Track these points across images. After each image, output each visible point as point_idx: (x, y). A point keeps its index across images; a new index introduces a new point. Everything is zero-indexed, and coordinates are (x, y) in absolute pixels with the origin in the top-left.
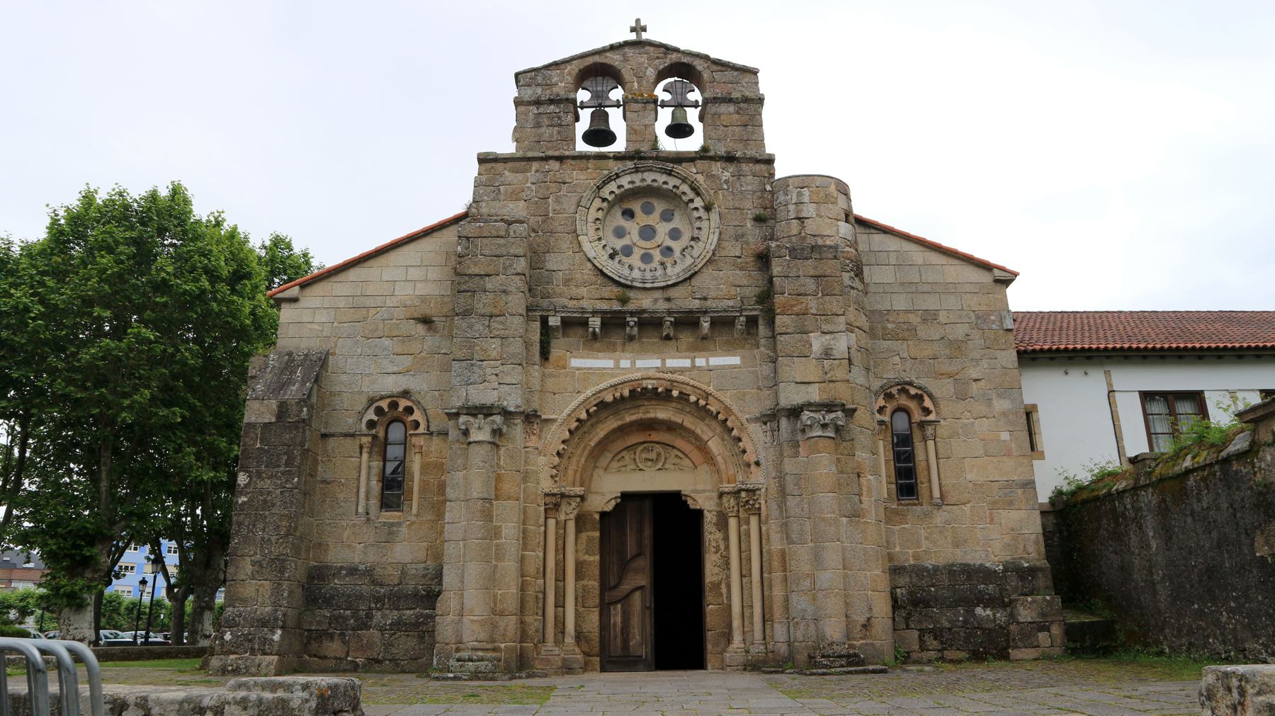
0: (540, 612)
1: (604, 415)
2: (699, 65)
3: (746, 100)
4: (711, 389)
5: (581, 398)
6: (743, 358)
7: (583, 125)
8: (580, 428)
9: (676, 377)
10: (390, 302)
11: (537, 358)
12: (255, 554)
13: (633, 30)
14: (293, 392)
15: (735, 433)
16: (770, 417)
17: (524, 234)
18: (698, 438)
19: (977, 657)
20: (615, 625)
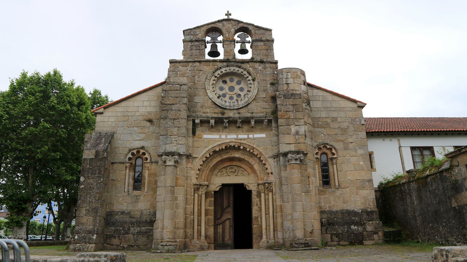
0: (192, 228)
1: (216, 155)
2: (251, 28)
3: (268, 41)
4: (255, 146)
5: (207, 149)
6: (266, 135)
7: (208, 49)
8: (207, 160)
9: (242, 141)
10: (137, 114)
11: (191, 135)
12: (87, 206)
13: (226, 15)
14: (101, 147)
15: (263, 162)
16: (276, 156)
17: (186, 89)
18: (250, 164)
19: (352, 244)
20: (219, 232)
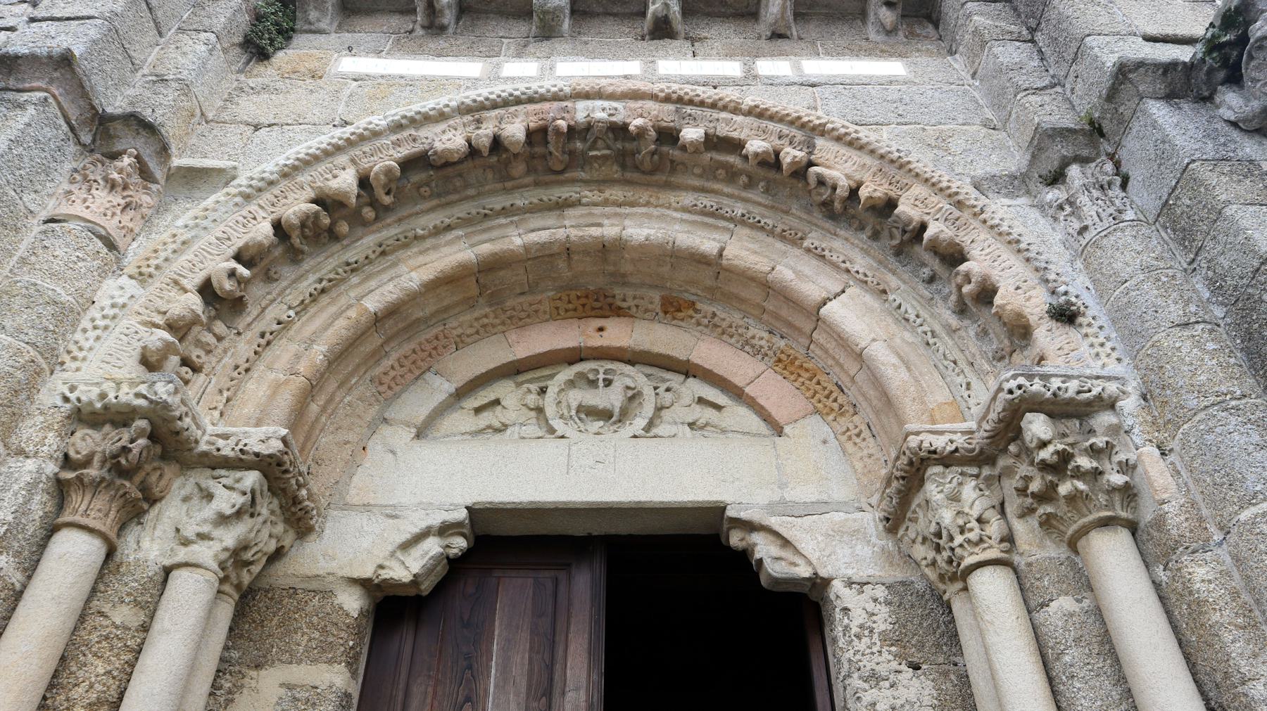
16: (1079, 148)
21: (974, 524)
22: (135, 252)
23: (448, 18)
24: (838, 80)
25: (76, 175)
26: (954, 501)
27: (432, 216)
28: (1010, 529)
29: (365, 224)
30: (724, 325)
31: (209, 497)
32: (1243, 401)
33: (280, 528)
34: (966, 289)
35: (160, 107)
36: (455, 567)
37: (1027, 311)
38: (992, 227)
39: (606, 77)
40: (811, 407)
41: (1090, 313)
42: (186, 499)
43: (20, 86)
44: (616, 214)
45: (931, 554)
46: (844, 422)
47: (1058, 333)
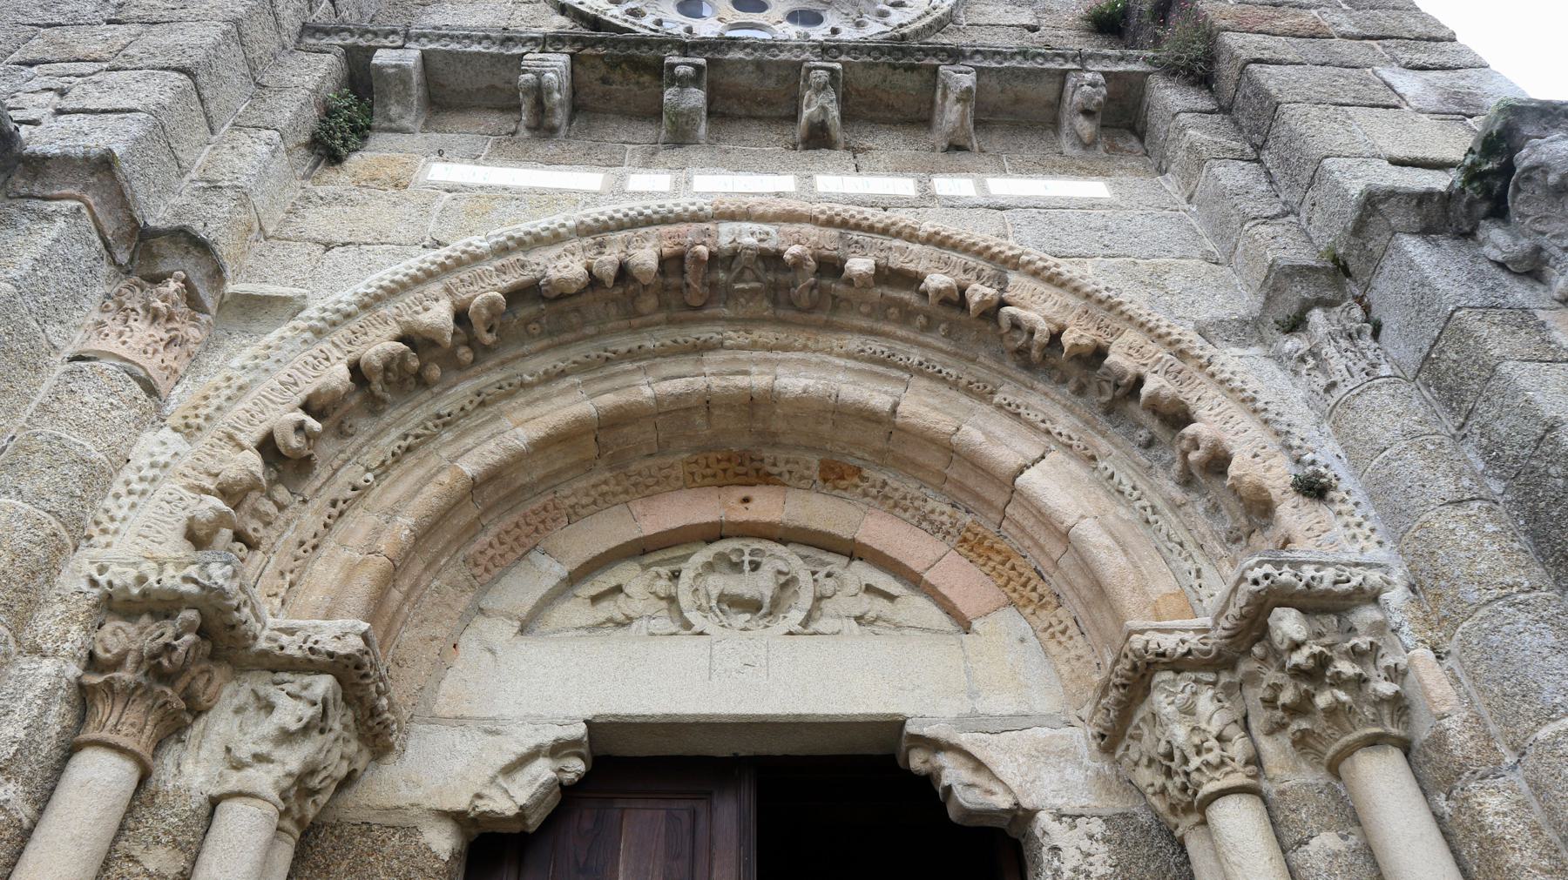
16: (1322, 288)
21: (1213, 743)
22: (180, 398)
23: (560, 118)
24: (1031, 203)
25: (109, 302)
26: (1188, 714)
27: (542, 358)
28: (1257, 749)
29: (460, 367)
30: (897, 496)
31: (269, 707)
32: (1533, 595)
33: (354, 746)
34: (1193, 456)
35: (213, 220)
36: (568, 796)
37: (1267, 483)
38: (1222, 382)
39: (754, 194)
40: (1004, 598)
41: (1343, 486)
42: (239, 710)
43: (48, 193)
44: (767, 360)
45: (1159, 780)
46: (1045, 616)
47: (1305, 510)
